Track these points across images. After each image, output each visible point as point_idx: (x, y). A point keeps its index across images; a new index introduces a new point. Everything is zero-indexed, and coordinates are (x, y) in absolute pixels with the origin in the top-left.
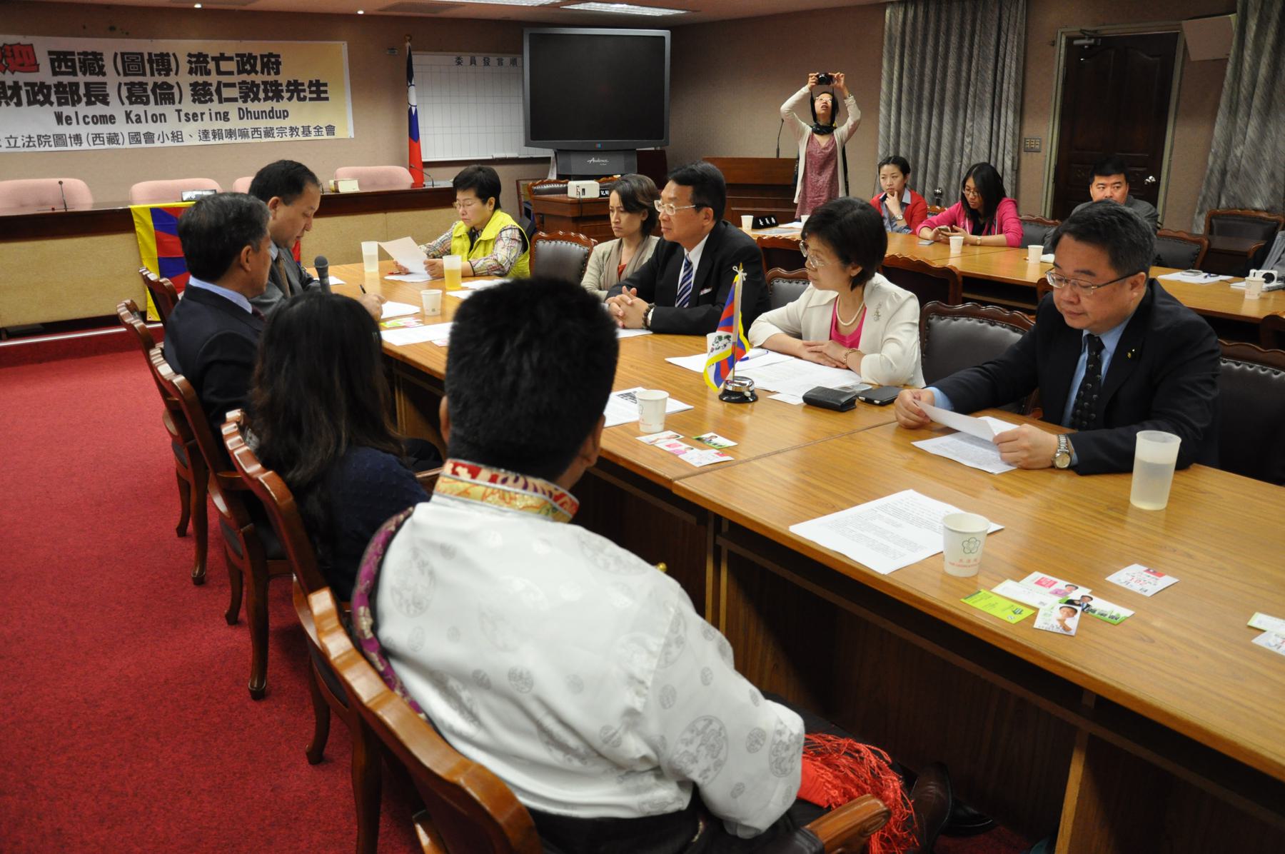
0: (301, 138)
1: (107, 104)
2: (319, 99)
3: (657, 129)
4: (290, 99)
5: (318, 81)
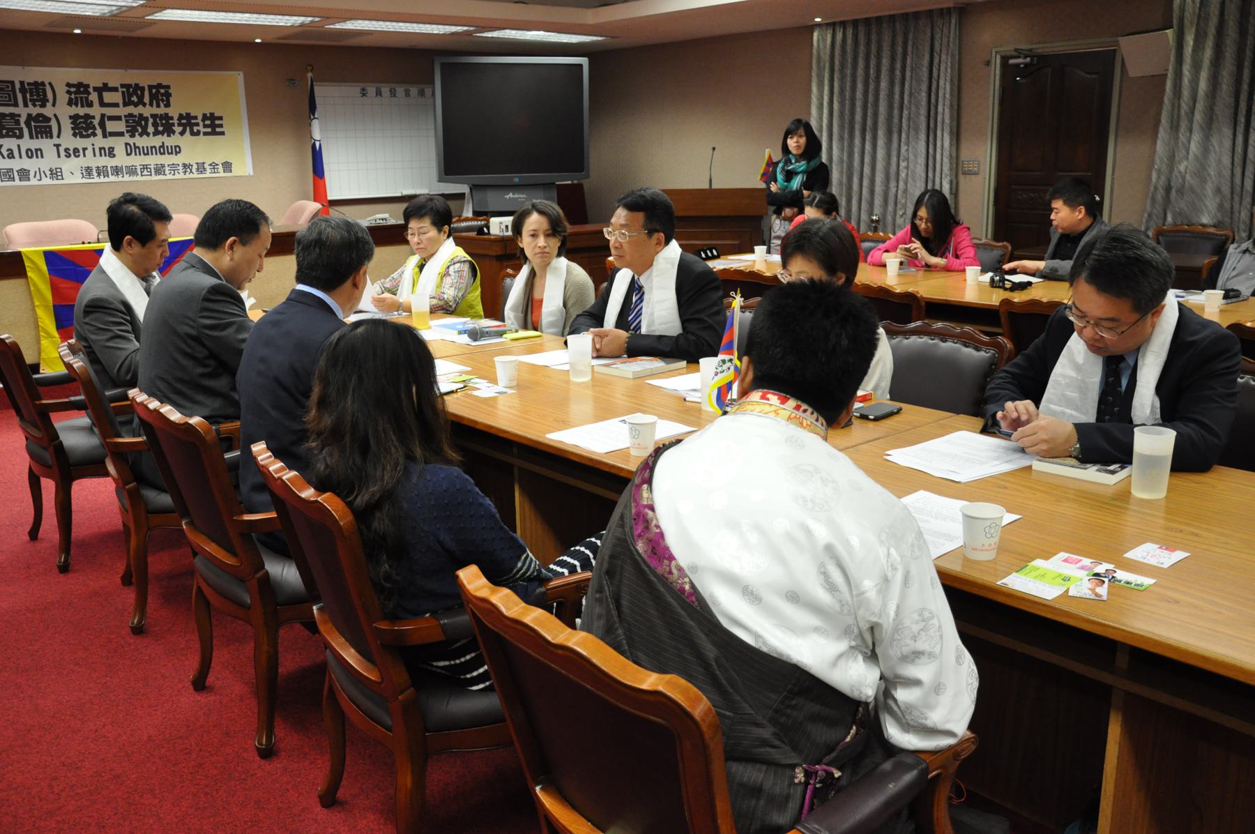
0: (195, 175)
2: (214, 133)
3: (575, 159)
4: (182, 133)
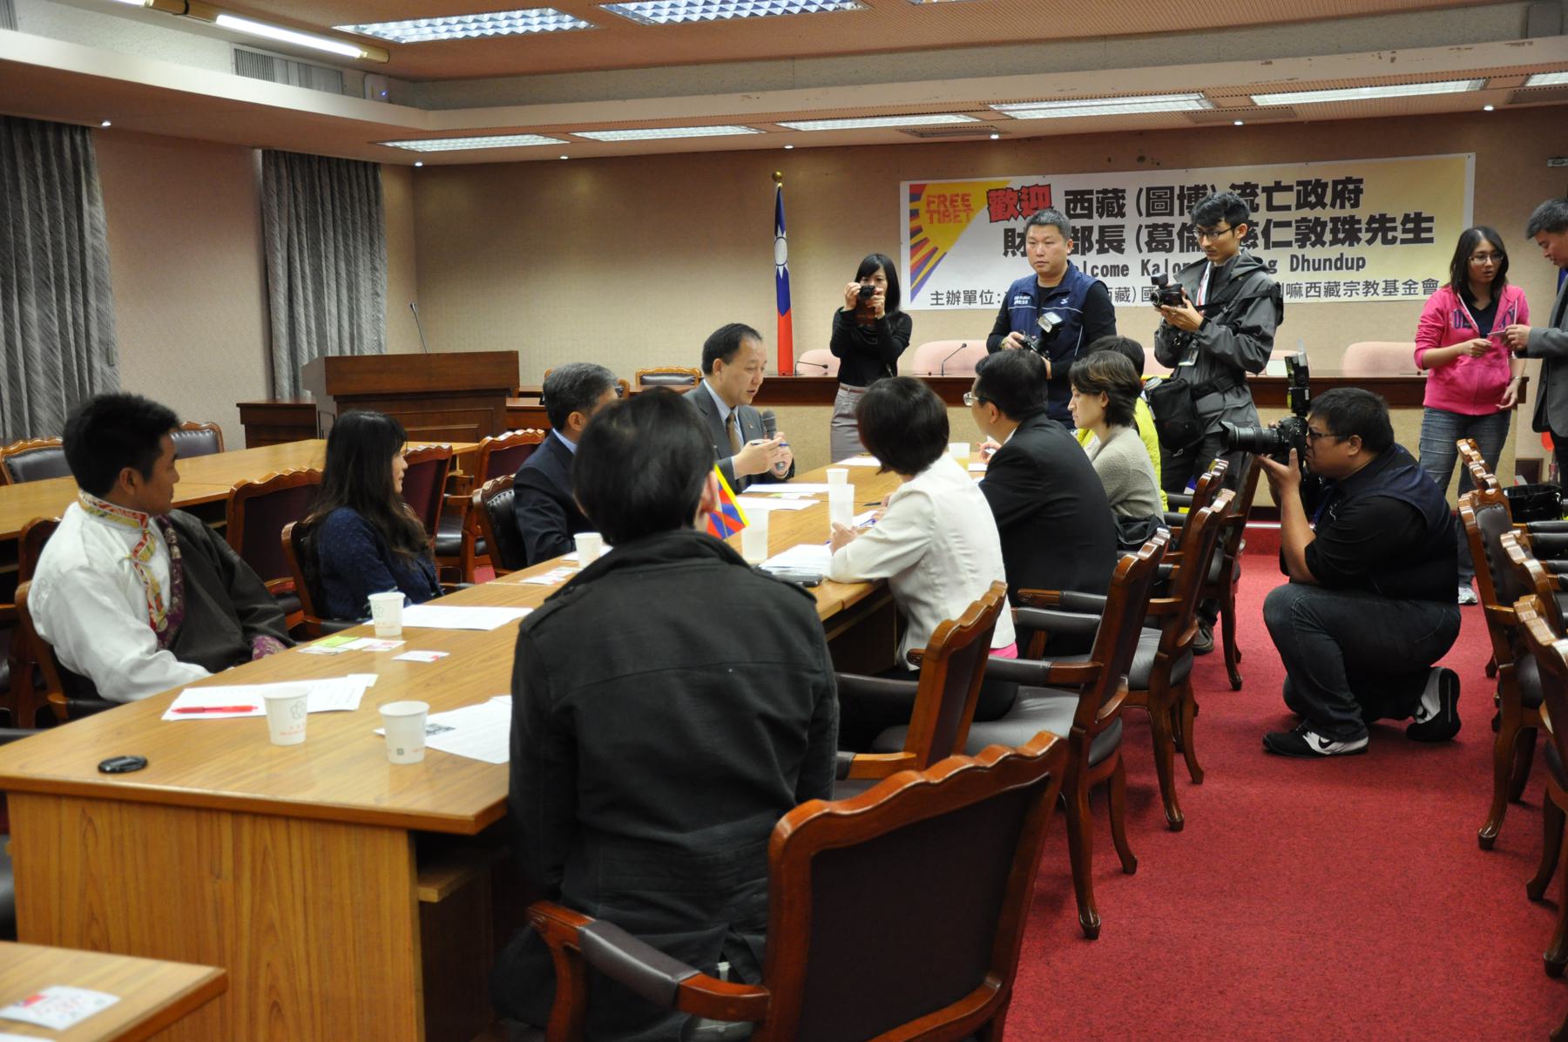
0: (1381, 297)
1: (1121, 251)
2: (1417, 240)
4: (1370, 242)
5: (1418, 215)
